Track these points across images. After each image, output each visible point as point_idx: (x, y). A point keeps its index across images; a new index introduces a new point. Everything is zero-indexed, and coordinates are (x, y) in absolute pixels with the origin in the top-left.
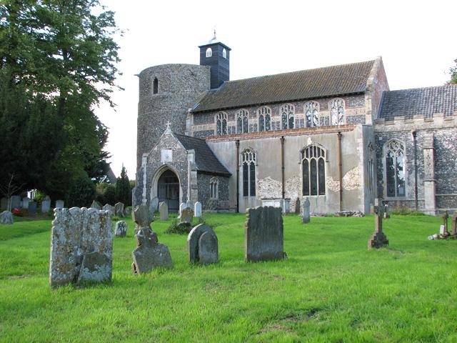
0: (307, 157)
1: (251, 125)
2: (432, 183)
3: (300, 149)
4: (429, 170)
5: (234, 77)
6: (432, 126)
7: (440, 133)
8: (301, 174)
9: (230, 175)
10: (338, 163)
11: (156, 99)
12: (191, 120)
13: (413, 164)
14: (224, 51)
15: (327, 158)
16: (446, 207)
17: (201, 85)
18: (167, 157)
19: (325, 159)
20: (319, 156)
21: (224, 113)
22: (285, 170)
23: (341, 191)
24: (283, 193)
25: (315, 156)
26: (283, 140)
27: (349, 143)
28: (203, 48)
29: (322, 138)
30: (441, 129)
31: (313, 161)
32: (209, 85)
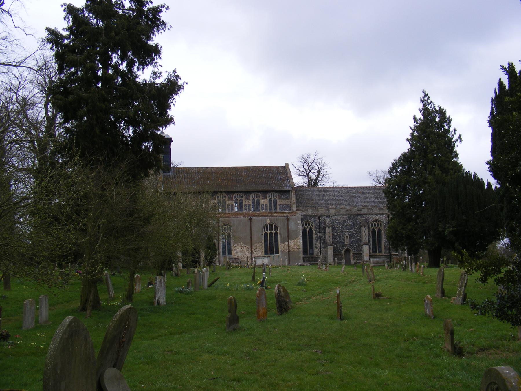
0: (267, 230)
3: (262, 226)
4: (329, 239)
7: (333, 218)
8: (263, 241)
10: (287, 235)
19: (278, 232)
20: (275, 230)
22: (253, 238)
23: (289, 252)
24: (252, 253)
26: (251, 219)
27: (293, 223)
30: (333, 216)
31: (271, 233)
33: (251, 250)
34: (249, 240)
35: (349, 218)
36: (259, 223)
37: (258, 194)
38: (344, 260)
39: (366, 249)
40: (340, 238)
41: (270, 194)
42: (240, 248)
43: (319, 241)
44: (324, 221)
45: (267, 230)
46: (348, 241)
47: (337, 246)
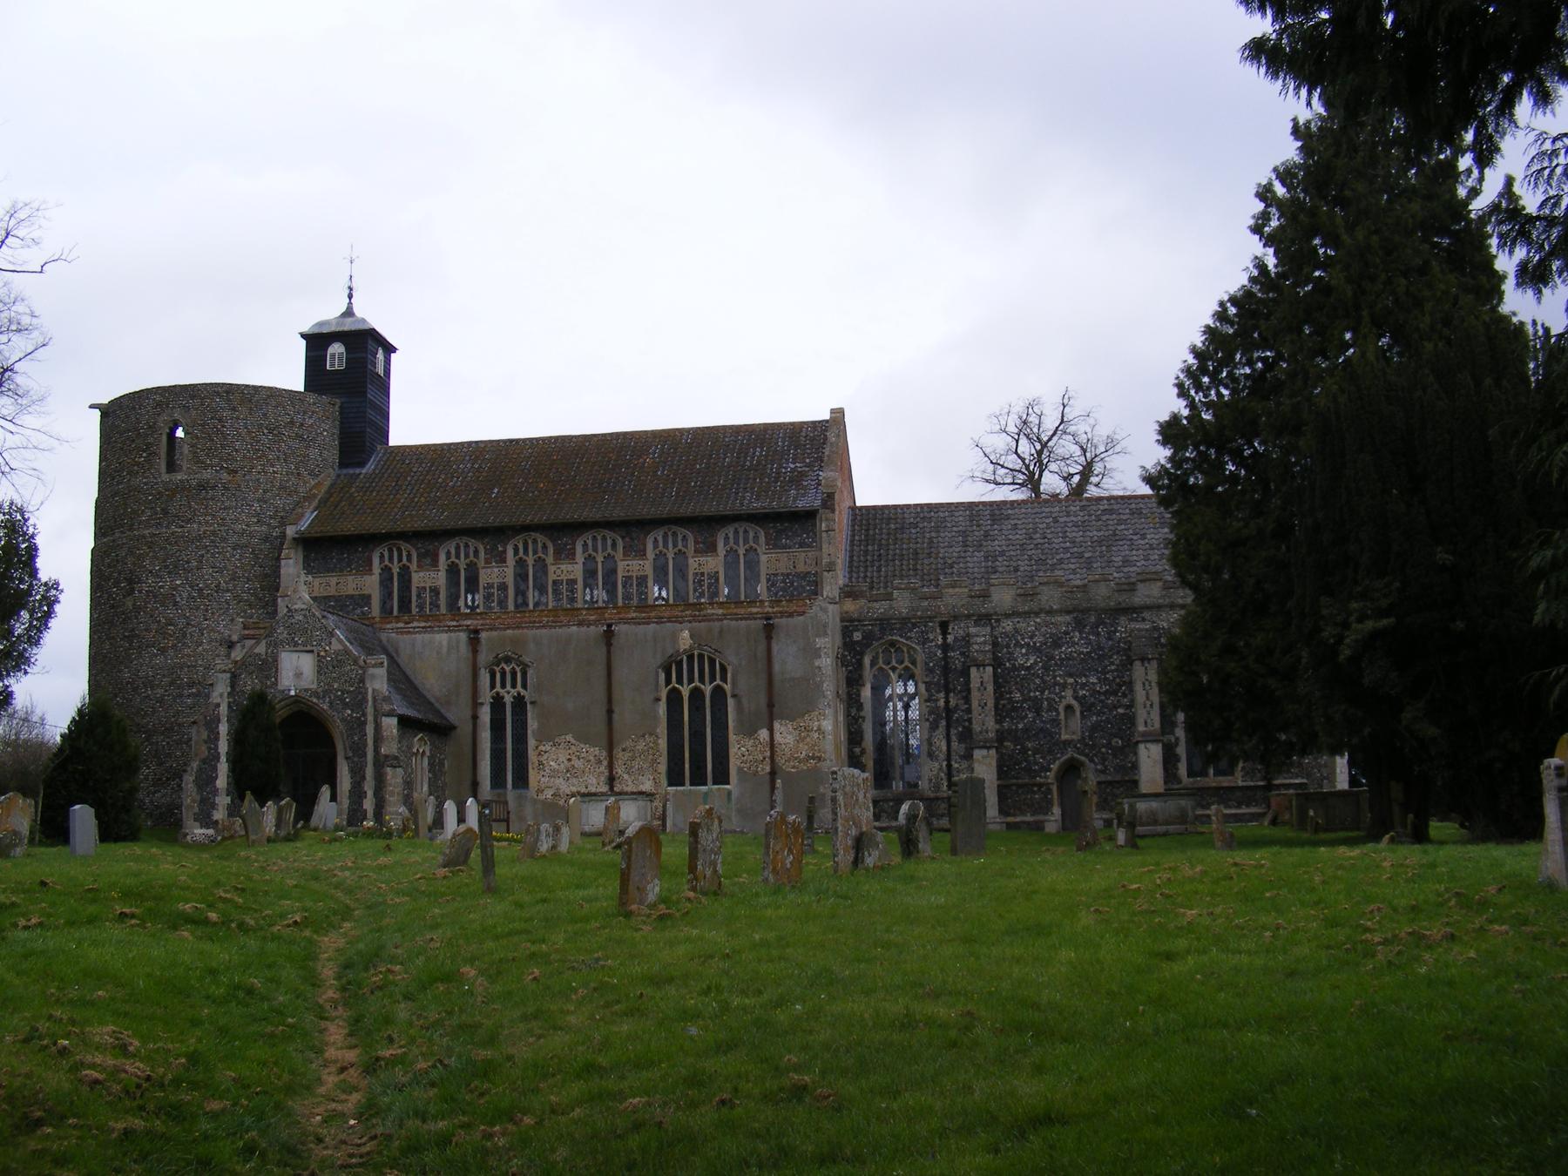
0: (680, 681)
1: (490, 586)
2: (993, 752)
3: (659, 660)
4: (985, 721)
5: (400, 435)
6: (987, 607)
7: (1008, 625)
8: (662, 729)
9: (453, 728)
10: (763, 701)
11: (182, 488)
13: (942, 703)
14: (380, 355)
15: (734, 684)
16: (1023, 813)
17: (314, 453)
18: (299, 675)
19: (727, 687)
20: (713, 679)
21: (404, 546)
22: (616, 716)
25: (702, 680)
26: (609, 635)
28: (316, 342)
29: (721, 632)
30: (1007, 616)
31: (696, 694)
32: (333, 455)
33: (611, 766)
34: (601, 727)
35: (1079, 625)
36: (645, 648)
37: (681, 531)
38: (1057, 811)
39: (1149, 759)
40: (1038, 711)
41: (730, 530)
42: (563, 758)
43: (941, 730)
44: (966, 640)
45: (680, 681)
46: (1072, 729)
47: (1024, 750)
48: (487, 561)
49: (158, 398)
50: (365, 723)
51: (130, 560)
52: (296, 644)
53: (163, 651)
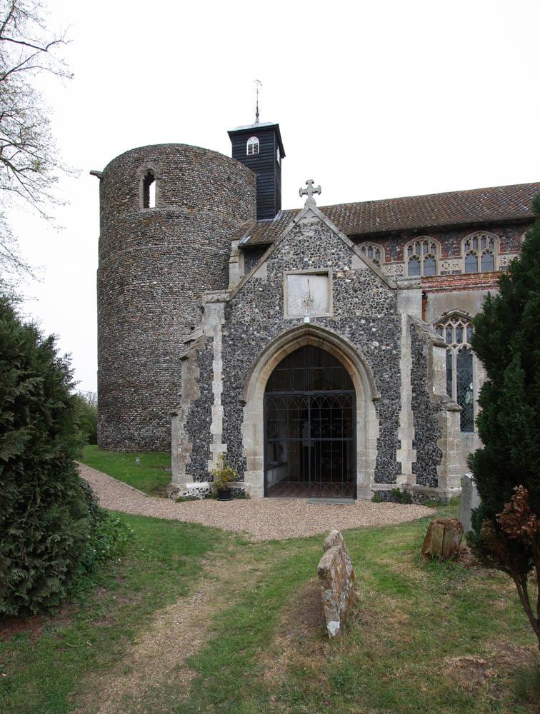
5: (283, 208)
12: (240, 266)
18: (309, 302)
32: (253, 209)
48: (388, 260)
49: (136, 155)
50: (397, 357)
51: (121, 269)
52: (305, 265)
53: (145, 331)
